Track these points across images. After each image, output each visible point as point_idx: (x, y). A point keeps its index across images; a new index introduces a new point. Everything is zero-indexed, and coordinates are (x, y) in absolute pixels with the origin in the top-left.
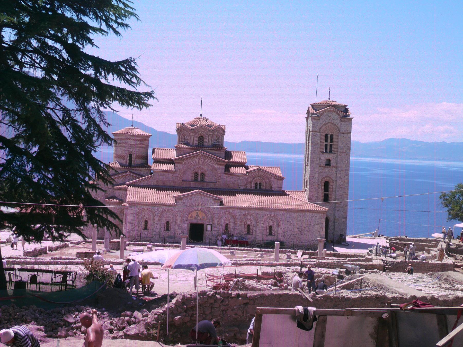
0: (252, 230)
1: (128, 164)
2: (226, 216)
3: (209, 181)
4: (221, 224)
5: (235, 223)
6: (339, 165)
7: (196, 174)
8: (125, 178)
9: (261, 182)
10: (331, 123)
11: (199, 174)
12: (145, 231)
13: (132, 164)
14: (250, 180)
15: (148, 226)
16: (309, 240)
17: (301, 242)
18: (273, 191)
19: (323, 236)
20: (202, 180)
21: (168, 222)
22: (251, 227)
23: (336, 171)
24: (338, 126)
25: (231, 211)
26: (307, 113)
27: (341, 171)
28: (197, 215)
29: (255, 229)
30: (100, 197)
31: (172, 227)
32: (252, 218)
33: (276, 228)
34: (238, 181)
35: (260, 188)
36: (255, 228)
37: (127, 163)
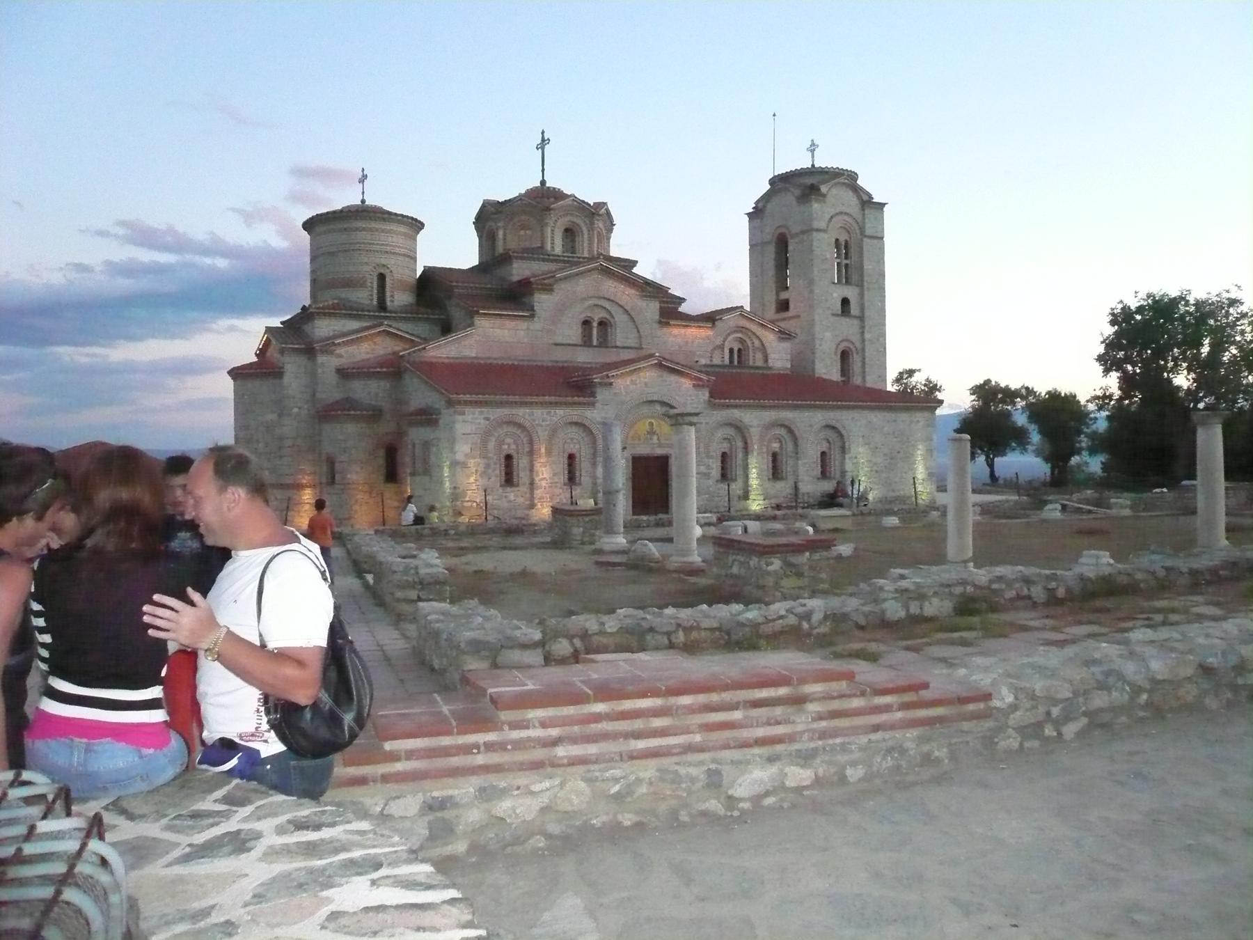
0: (787, 466)
1: (375, 302)
2: (720, 434)
3: (625, 345)
4: (712, 454)
5: (746, 450)
6: (867, 313)
7: (586, 323)
8: (375, 343)
9: (740, 346)
10: (846, 214)
11: (595, 324)
12: (509, 489)
13: (388, 304)
14: (719, 341)
17: (893, 491)
18: (770, 368)
20: (604, 343)
21: (571, 457)
23: (863, 327)
27: (870, 328)
28: (651, 432)
30: (299, 405)
33: (838, 456)
34: (693, 342)
35: (739, 362)
37: (372, 300)
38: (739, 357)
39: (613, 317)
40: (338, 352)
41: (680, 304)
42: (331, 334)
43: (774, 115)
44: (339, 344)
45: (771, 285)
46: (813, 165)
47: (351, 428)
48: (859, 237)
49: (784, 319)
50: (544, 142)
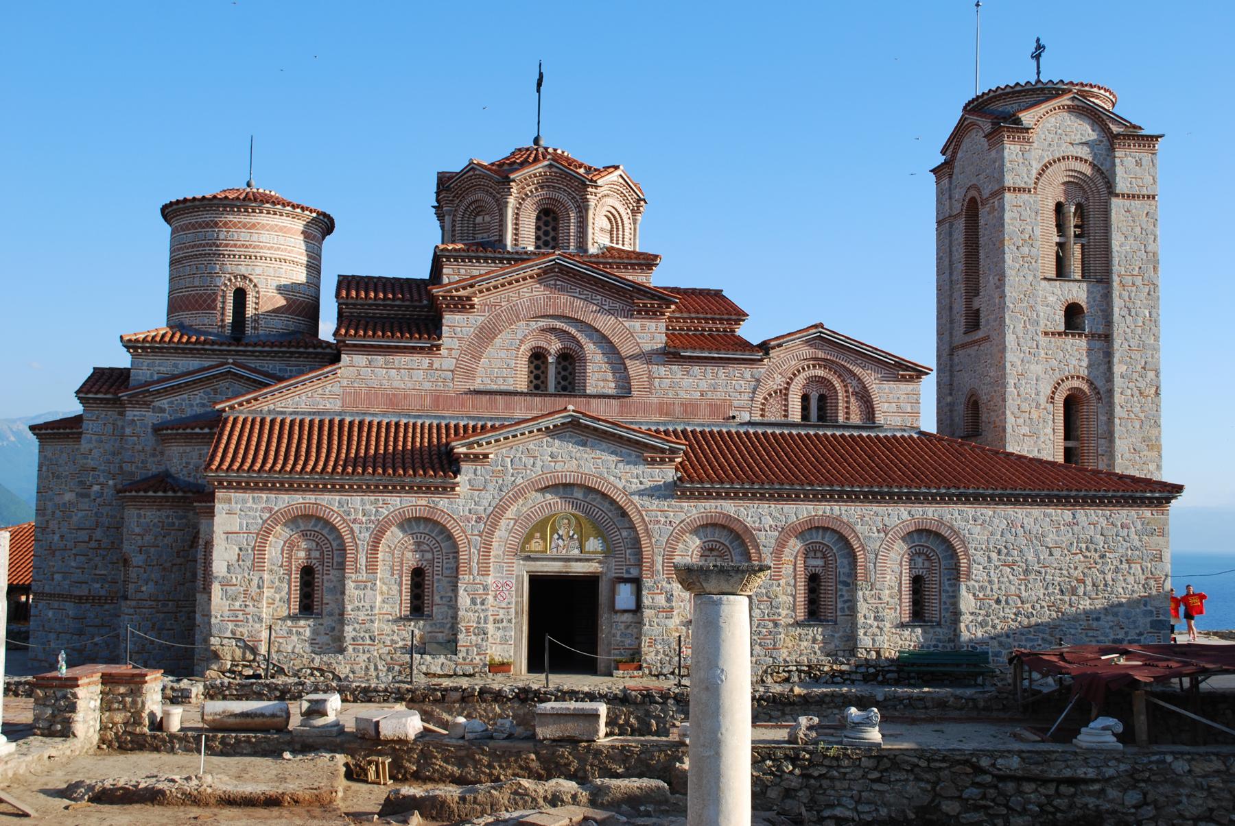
1: (228, 331)
7: (538, 357)
8: (215, 391)
14: (778, 381)
15: (317, 596)
16: (1101, 638)
18: (880, 427)
19: (1162, 618)
22: (828, 585)
24: (1104, 169)
25: (729, 507)
26: (943, 152)
29: (846, 598)
30: (102, 480)
31: (437, 599)
32: (828, 539)
35: (822, 417)
36: (845, 588)
38: (822, 409)
39: (581, 347)
40: (157, 404)
41: (738, 322)
42: (155, 377)
43: (977, 5)
44: (158, 392)
45: (961, 288)
46: (1038, 81)
47: (151, 515)
48: (1104, 196)
49: (974, 343)
50: (539, 84)
